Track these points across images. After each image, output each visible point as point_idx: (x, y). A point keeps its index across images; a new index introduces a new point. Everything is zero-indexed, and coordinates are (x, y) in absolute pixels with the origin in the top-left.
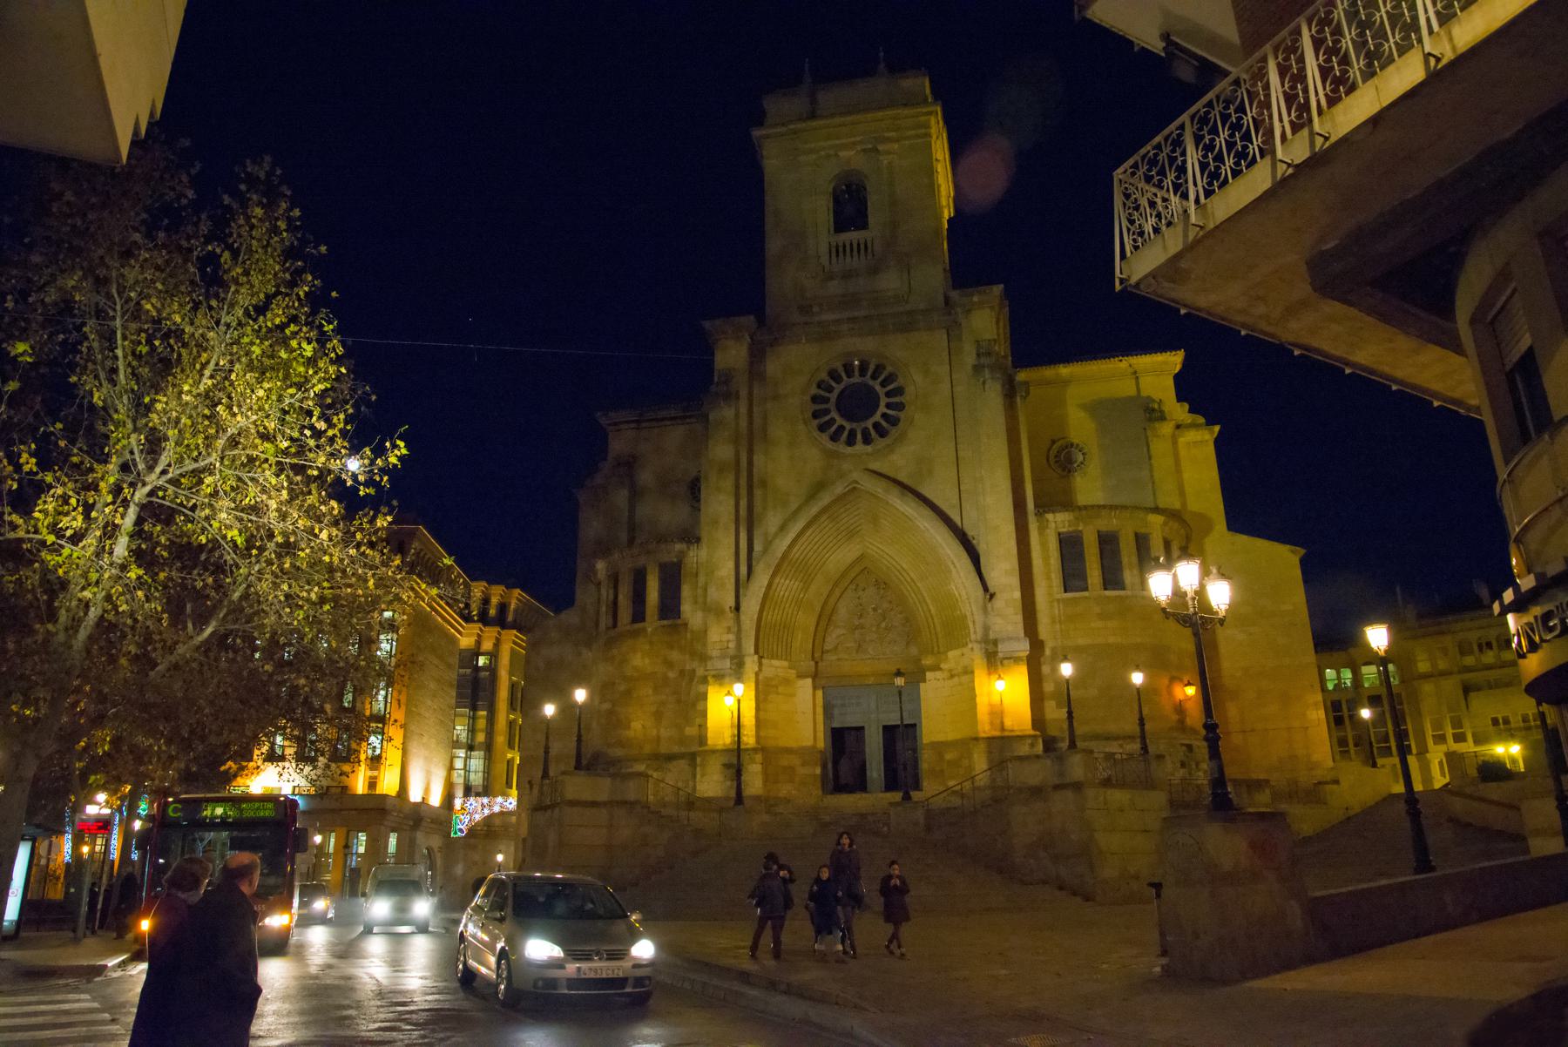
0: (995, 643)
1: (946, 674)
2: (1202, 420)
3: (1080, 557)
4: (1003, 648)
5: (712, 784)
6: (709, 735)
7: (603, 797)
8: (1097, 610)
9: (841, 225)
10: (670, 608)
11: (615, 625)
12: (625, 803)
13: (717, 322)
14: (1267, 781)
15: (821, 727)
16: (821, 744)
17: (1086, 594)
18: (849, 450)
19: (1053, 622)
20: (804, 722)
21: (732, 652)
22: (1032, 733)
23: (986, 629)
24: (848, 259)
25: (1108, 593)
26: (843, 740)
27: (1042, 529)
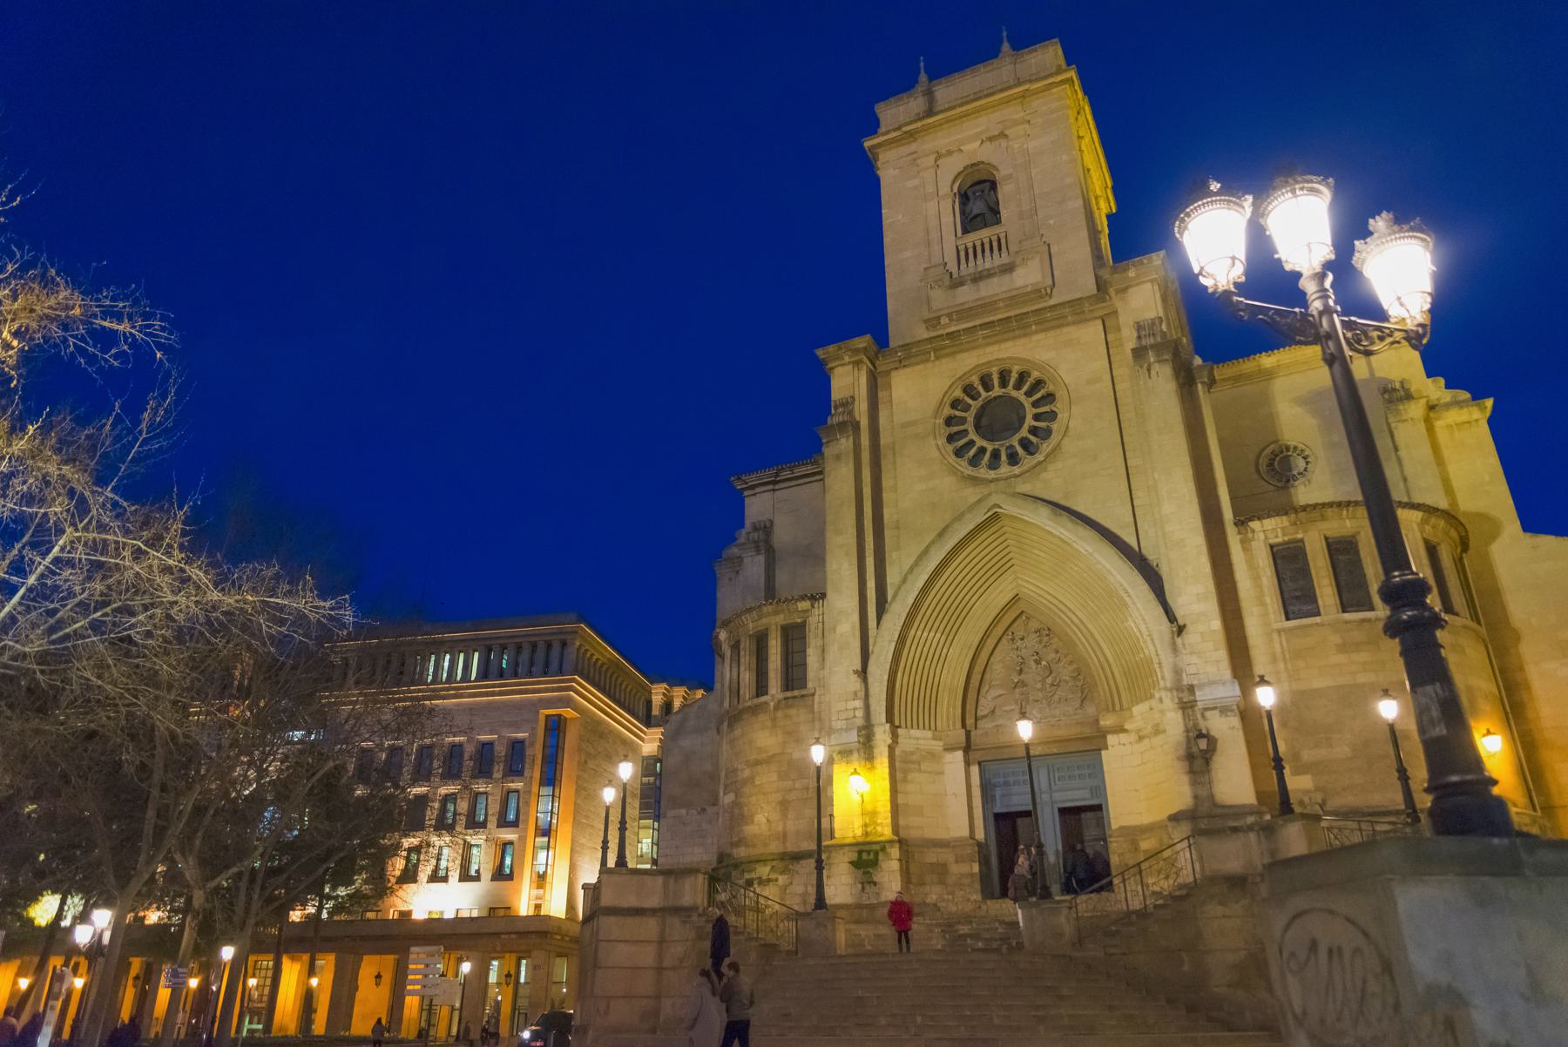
0: (1191, 689)
1: (1133, 737)
3: (1305, 572)
6: (837, 825)
9: (970, 223)
10: (794, 677)
13: (831, 348)
16: (980, 835)
17: (1318, 619)
18: (992, 474)
20: (954, 808)
23: (1178, 672)
25: (1347, 616)
26: (1009, 828)
27: (1245, 543)
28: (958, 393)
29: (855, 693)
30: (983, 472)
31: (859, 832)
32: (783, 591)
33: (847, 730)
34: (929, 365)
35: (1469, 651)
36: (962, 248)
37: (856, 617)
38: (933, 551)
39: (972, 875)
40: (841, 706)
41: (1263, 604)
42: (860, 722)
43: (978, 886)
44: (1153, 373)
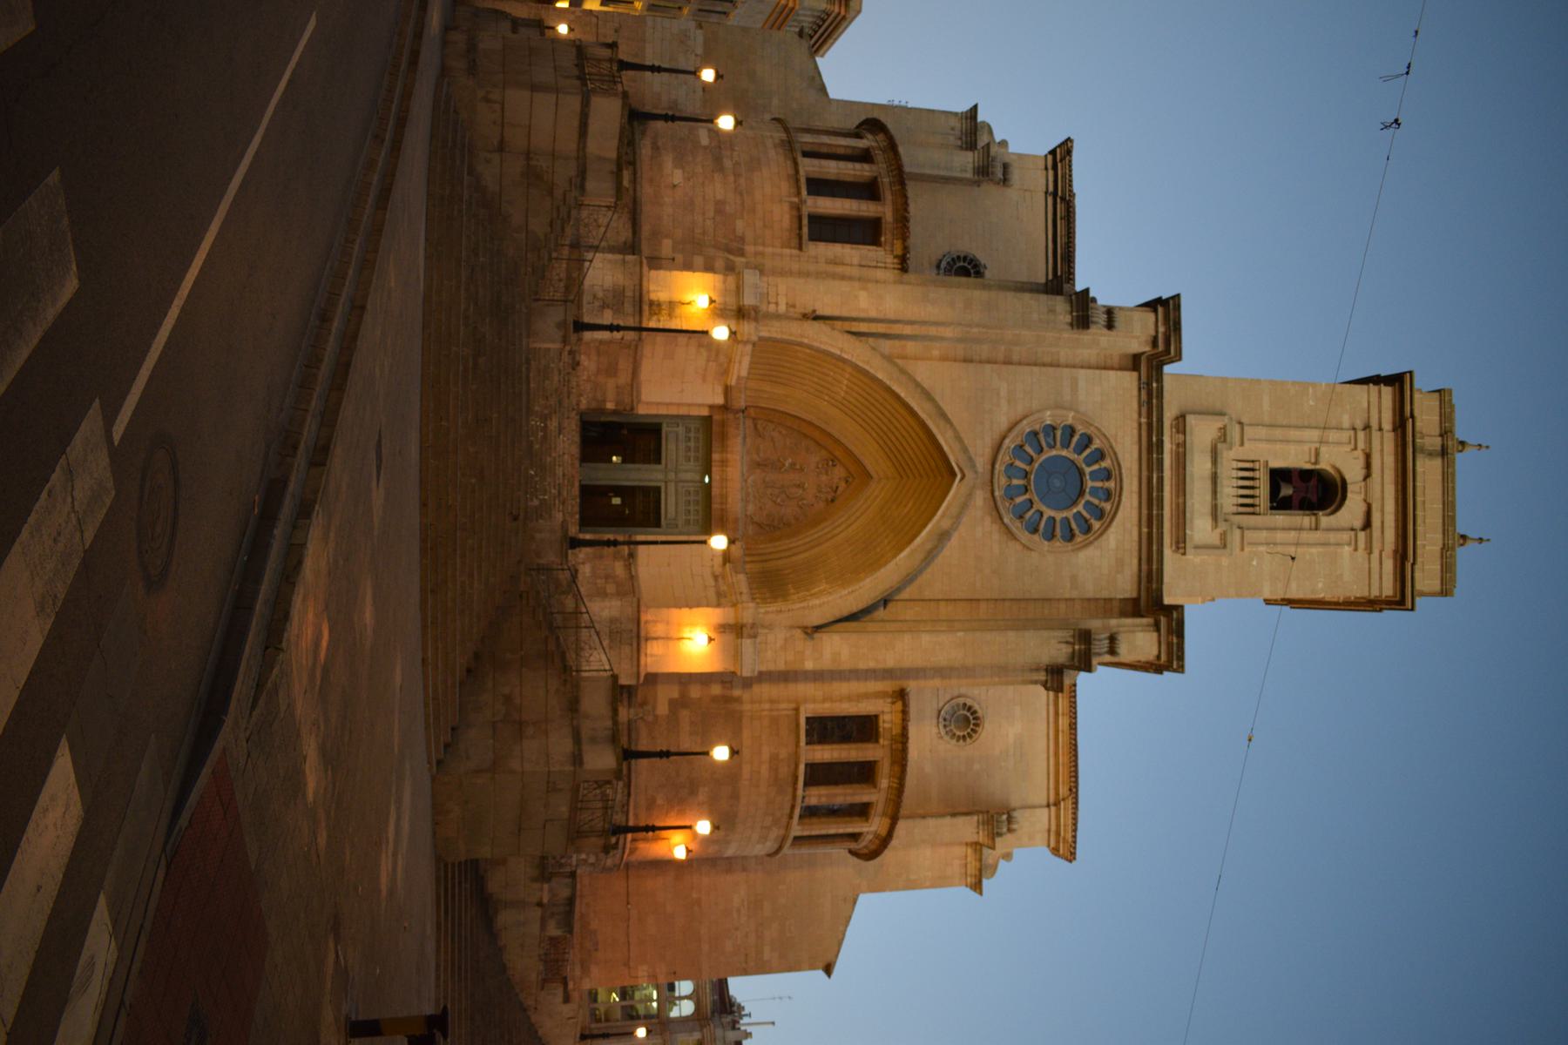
1: (718, 570)
3: (846, 739)
4: (747, 643)
5: (602, 273)
6: (662, 272)
7: (592, 147)
10: (826, 229)
11: (806, 154)
12: (582, 174)
14: (571, 932)
15: (663, 411)
16: (642, 410)
19: (772, 701)
20: (669, 390)
21: (764, 307)
23: (770, 627)
24: (1235, 474)
25: (802, 768)
28: (1096, 444)
29: (794, 306)
31: (653, 296)
34: (1135, 416)
35: (759, 847)
36: (1257, 466)
37: (873, 314)
38: (928, 406)
39: (604, 401)
40: (782, 288)
41: (824, 700)
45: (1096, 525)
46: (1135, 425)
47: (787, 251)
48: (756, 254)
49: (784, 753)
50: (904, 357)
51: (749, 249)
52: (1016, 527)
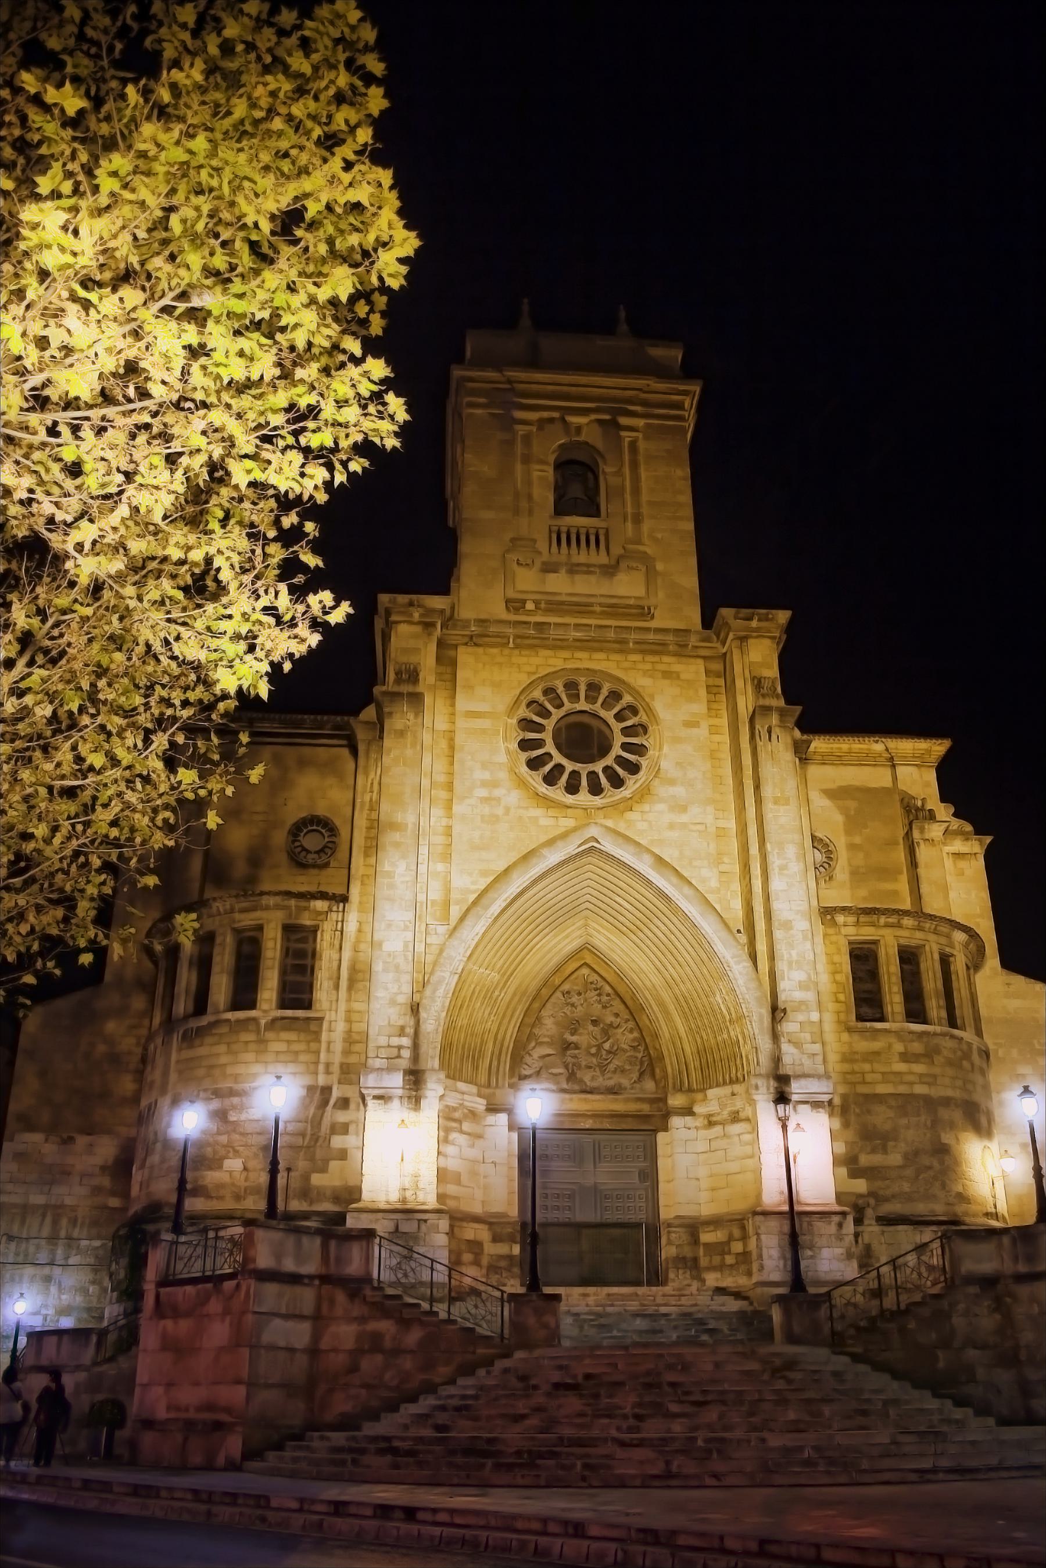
1: (700, 1122)
2: (969, 828)
8: (899, 1047)
13: (402, 599)
18: (570, 799)
22: (837, 1208)
29: (402, 1028)
30: (557, 793)
32: (339, 890)
33: (390, 1069)
34: (506, 652)
36: (555, 529)
38: (515, 875)
39: (510, 1257)
40: (383, 1041)
42: (405, 1063)
43: (516, 1270)
44: (774, 737)
45: (627, 699)
46: (516, 652)
47: (324, 1036)
48: (328, 1072)
49: (899, 1047)
50: (447, 904)
51: (322, 1080)
52: (633, 784)
